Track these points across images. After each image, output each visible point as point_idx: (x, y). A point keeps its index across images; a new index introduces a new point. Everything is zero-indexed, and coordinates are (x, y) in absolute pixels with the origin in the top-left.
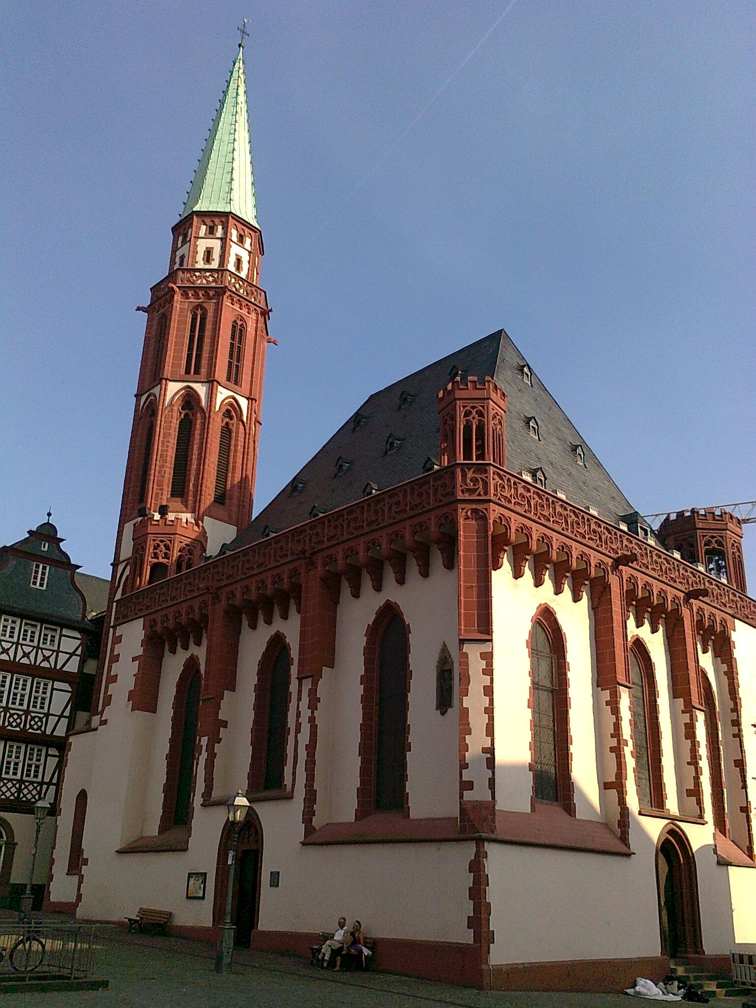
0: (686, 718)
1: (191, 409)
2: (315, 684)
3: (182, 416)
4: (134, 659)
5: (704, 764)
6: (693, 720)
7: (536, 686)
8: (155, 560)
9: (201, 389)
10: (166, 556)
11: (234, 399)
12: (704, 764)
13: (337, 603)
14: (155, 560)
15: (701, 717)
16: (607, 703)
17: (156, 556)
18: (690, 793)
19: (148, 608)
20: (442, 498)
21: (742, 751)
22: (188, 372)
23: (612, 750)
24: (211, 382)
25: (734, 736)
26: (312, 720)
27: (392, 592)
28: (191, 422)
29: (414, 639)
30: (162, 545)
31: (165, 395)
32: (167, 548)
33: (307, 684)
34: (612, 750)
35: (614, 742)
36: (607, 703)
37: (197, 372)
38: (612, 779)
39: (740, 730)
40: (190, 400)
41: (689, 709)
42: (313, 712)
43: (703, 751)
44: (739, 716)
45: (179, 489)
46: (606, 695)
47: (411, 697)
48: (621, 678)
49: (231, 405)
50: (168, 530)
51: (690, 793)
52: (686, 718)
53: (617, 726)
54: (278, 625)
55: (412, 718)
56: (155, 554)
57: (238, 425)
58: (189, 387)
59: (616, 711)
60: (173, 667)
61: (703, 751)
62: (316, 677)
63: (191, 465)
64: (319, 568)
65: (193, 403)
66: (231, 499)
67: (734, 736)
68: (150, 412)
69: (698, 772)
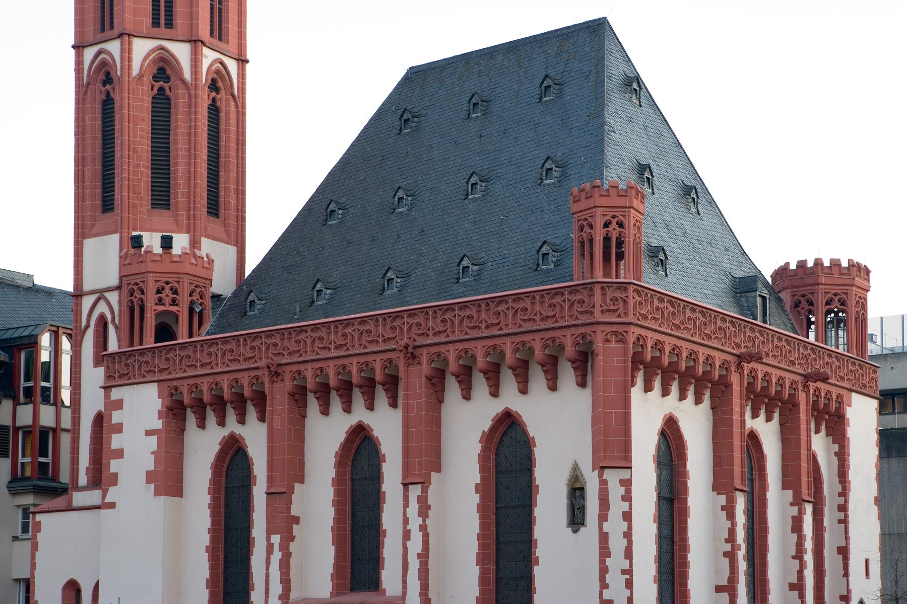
0: (794, 511)
1: (167, 79)
2: (425, 491)
3: (155, 90)
4: (149, 433)
5: (809, 558)
6: (801, 512)
7: (660, 498)
8: (161, 308)
9: (181, 51)
10: (174, 302)
11: (222, 63)
12: (809, 558)
13: (441, 401)
14: (161, 308)
15: (809, 508)
16: (723, 508)
17: (160, 302)
18: (792, 587)
19: (161, 371)
20: (579, 316)
21: (847, 538)
22: (156, 23)
23: (726, 554)
24: (195, 42)
25: (840, 521)
26: (423, 528)
27: (510, 398)
28: (168, 99)
29: (539, 453)
30: (167, 287)
31: (130, 60)
32: (175, 292)
33: (415, 491)
34: (726, 554)
35: (728, 547)
36: (723, 508)
37: (170, 24)
38: (725, 582)
39: (846, 516)
40: (163, 69)
41: (798, 501)
42: (424, 521)
43: (809, 545)
44: (846, 501)
45: (161, 196)
46: (722, 500)
47: (537, 512)
48: (737, 483)
49: (218, 72)
50: (173, 268)
51: (792, 587)
52: (794, 511)
53: (732, 532)
54: (360, 414)
55: (539, 532)
56: (160, 300)
57: (227, 100)
58: (162, 48)
59: (731, 516)
60: (203, 445)
61: (809, 545)
62: (425, 484)
63: (176, 164)
64: (424, 366)
65: (169, 72)
66: (227, 209)
67: (840, 521)
68: (102, 76)
69: (802, 566)
